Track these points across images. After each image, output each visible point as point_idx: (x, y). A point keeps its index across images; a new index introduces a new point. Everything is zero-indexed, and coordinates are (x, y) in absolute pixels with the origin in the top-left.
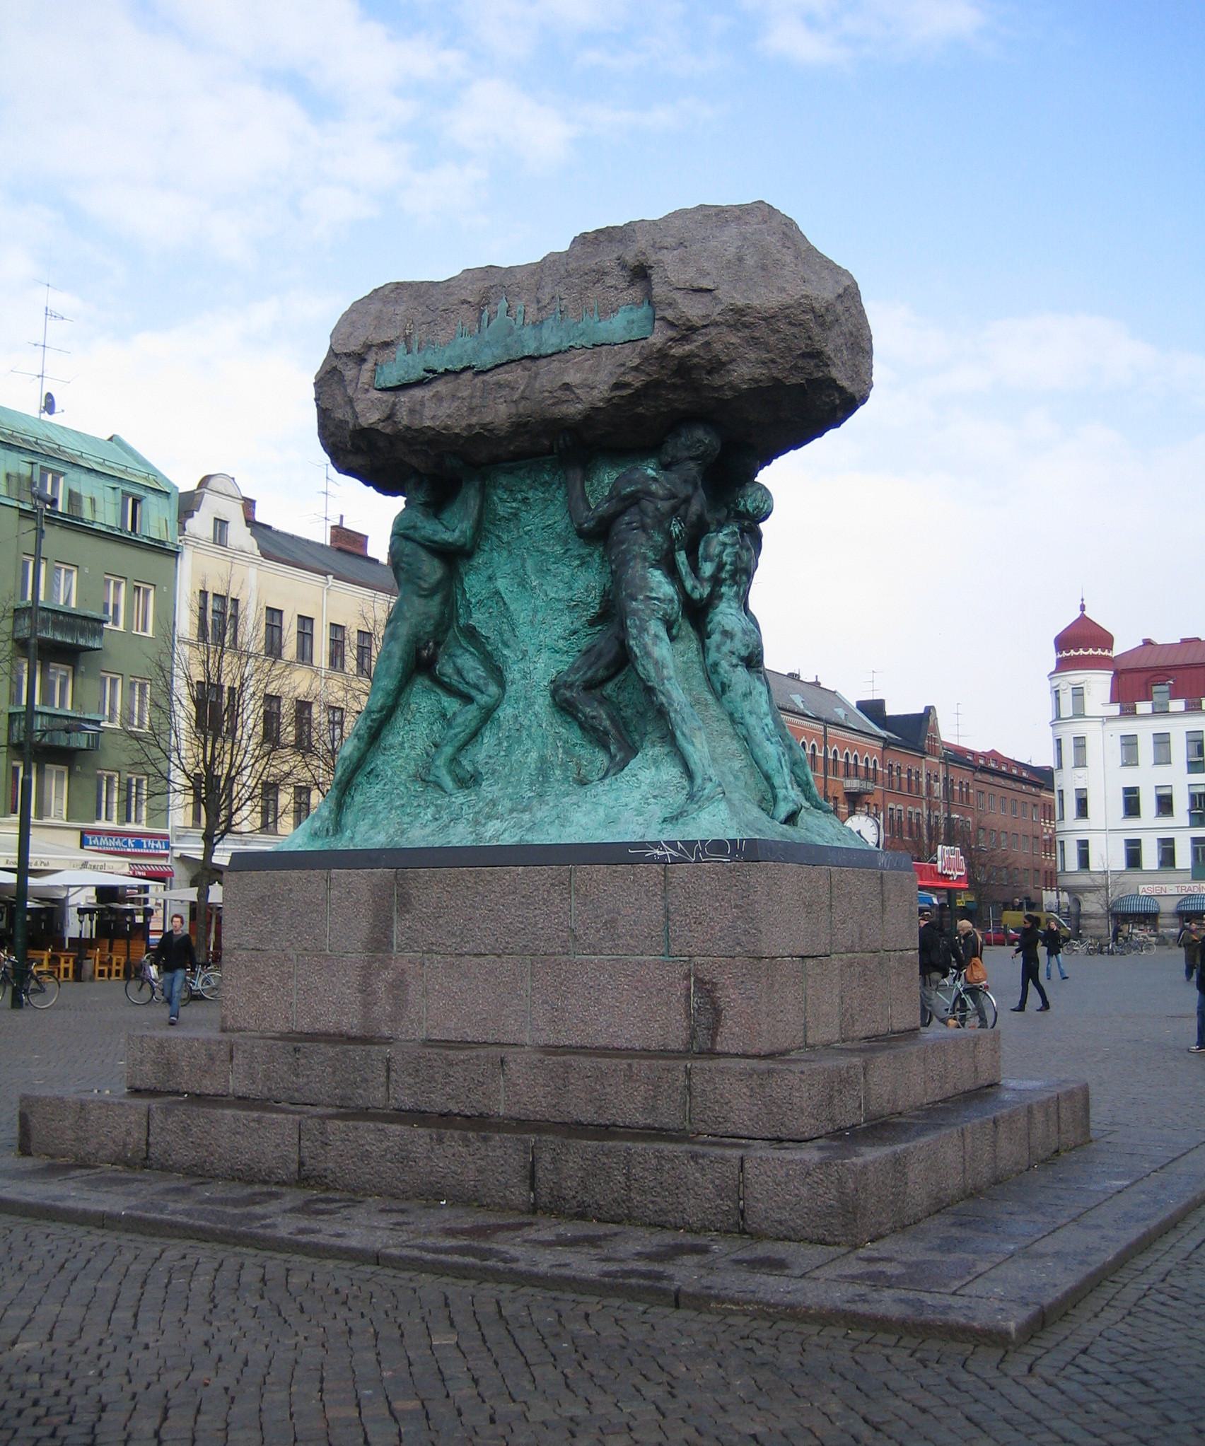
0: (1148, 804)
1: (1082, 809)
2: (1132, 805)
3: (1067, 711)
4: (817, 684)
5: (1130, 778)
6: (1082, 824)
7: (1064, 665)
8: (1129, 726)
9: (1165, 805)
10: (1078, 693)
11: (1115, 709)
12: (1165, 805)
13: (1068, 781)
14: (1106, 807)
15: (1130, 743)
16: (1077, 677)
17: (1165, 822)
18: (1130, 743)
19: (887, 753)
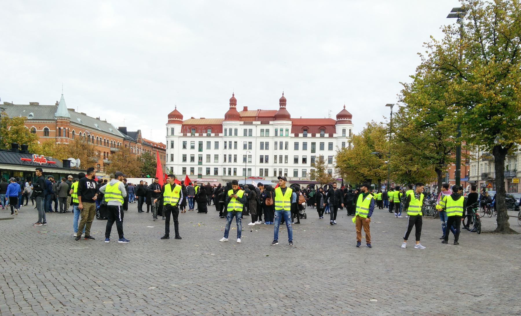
0: (188, 159)
1: (172, 160)
2: (185, 159)
3: (170, 134)
4: (105, 122)
5: (185, 152)
6: (172, 163)
7: (170, 122)
8: (185, 139)
9: (192, 159)
10: (173, 130)
11: (182, 134)
12: (192, 159)
13: (169, 151)
14: (178, 159)
17: (192, 163)
19: (125, 142)
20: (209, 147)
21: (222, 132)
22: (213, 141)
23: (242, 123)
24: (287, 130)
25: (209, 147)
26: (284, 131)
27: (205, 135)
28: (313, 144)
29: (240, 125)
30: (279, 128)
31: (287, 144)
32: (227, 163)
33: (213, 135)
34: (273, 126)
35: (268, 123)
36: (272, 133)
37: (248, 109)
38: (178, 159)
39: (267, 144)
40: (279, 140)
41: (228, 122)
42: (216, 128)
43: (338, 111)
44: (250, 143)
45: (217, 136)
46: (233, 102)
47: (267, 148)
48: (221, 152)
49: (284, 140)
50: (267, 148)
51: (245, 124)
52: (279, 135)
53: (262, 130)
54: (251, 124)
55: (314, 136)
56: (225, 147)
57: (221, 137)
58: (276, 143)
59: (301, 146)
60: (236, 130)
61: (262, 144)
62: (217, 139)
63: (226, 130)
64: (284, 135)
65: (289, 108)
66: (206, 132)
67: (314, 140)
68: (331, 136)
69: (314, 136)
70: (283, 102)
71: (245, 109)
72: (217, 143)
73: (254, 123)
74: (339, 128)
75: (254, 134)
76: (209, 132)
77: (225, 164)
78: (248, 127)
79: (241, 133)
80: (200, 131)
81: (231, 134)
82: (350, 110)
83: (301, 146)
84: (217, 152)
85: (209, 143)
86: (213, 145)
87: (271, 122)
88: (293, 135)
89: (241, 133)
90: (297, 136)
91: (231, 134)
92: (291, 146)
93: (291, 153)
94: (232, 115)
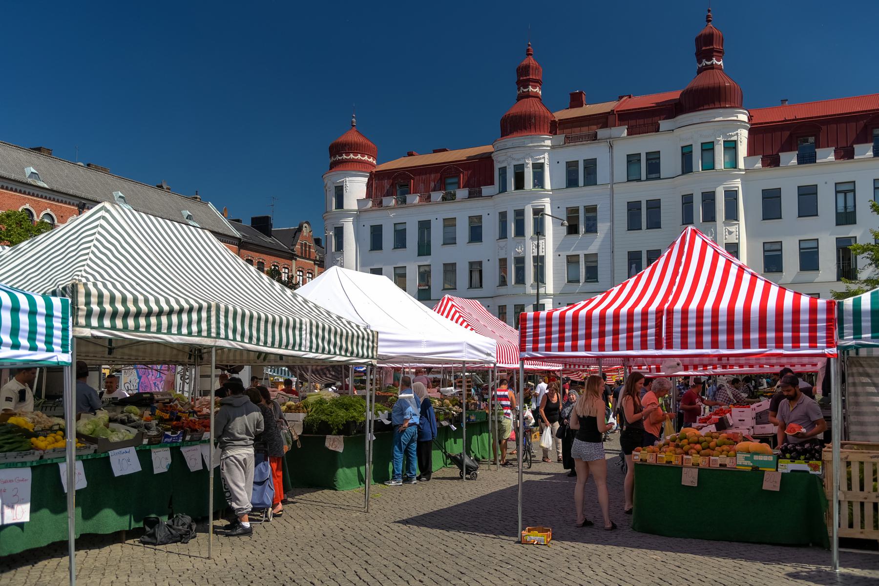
21: (492, 183)
28: (846, 190)
33: (462, 193)
35: (657, 130)
36: (670, 163)
39: (654, 206)
44: (591, 210)
45: (475, 194)
50: (655, 223)
55: (846, 154)
56: (503, 235)
58: (687, 201)
61: (633, 208)
62: (476, 207)
63: (503, 171)
67: (846, 171)
69: (846, 154)
73: (602, 133)
77: (503, 290)
85: (450, 223)
87: (664, 124)
90: (772, 161)
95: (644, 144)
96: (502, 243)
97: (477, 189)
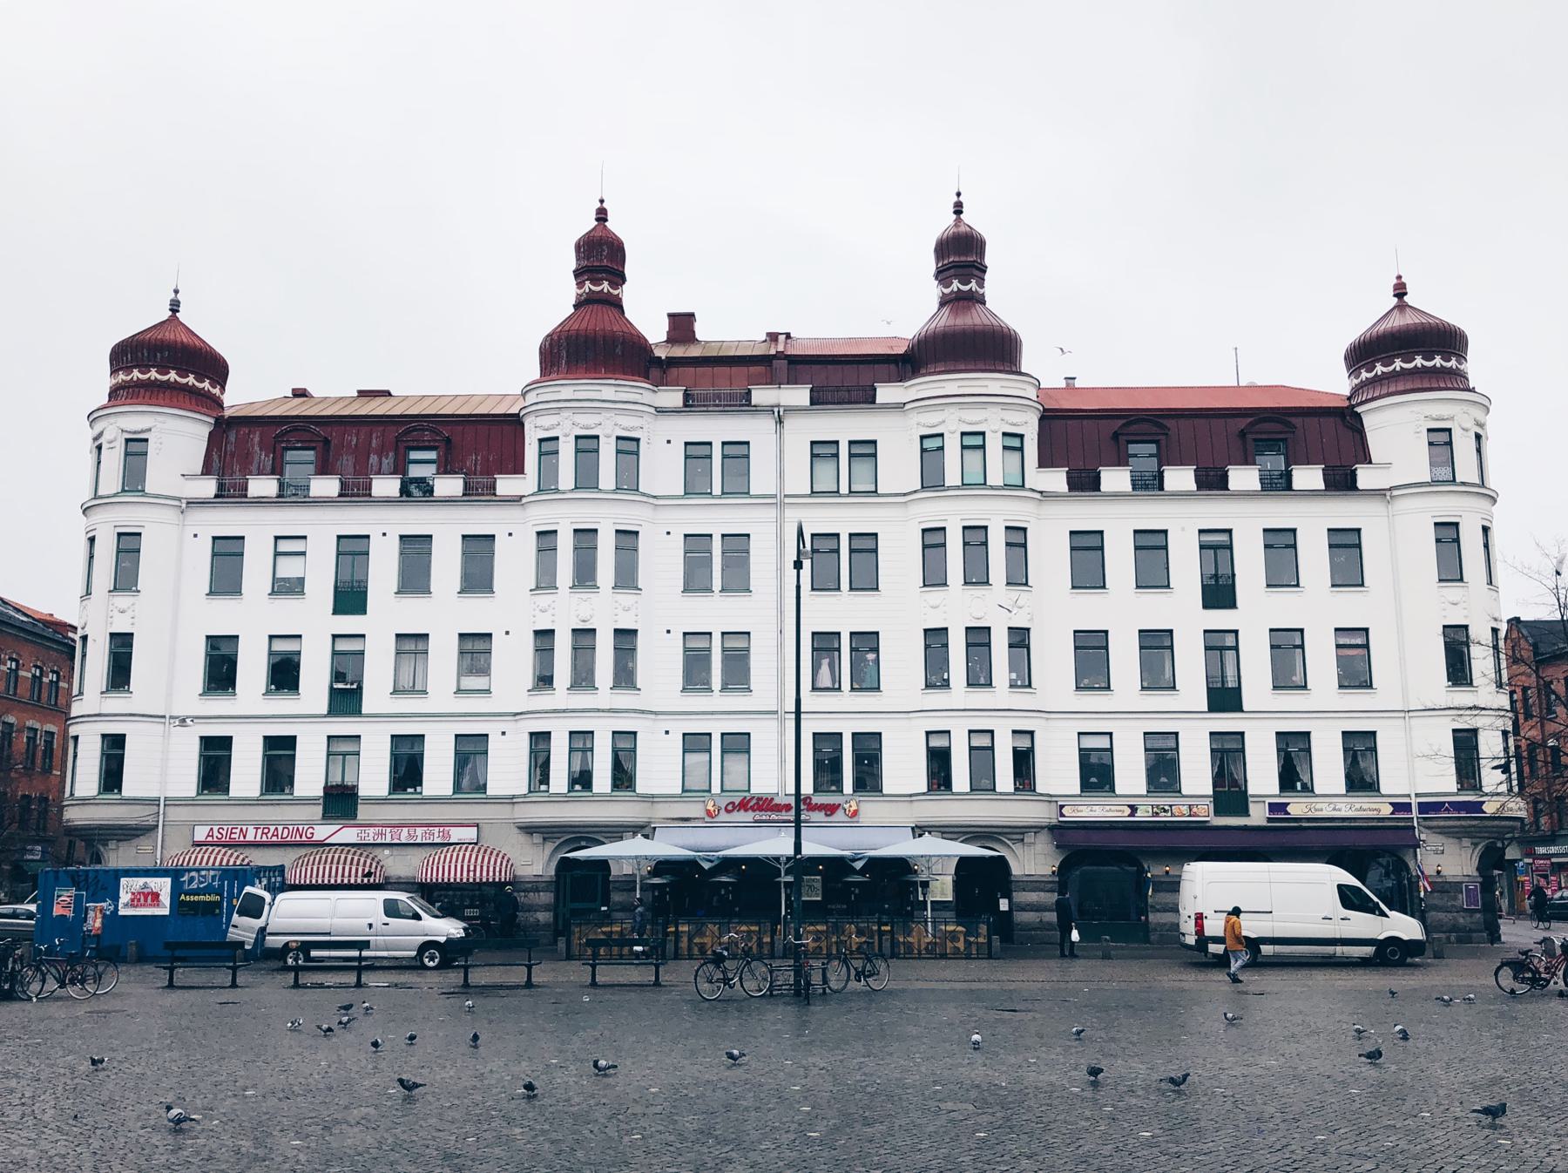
0: (252, 668)
1: (120, 674)
2: (221, 670)
3: (112, 481)
5: (223, 617)
6: (116, 703)
8: (229, 521)
9: (284, 674)
10: (136, 448)
11: (209, 487)
12: (284, 674)
14: (169, 673)
15: (228, 552)
16: (136, 419)
17: (283, 704)
18: (228, 552)
20: (414, 578)
21: (518, 468)
22: (447, 528)
23: (672, 397)
24: (1013, 441)
25: (414, 578)
26: (994, 445)
27: (385, 486)
28: (1217, 546)
29: (661, 411)
30: (952, 424)
31: (1017, 539)
32: (561, 694)
33: (448, 486)
34: (897, 424)
35: (869, 398)
36: (899, 465)
37: (701, 332)
38: (169, 673)
40: (953, 514)
41: (568, 390)
42: (479, 446)
43: (1367, 312)
45: (479, 491)
46: (601, 258)
47: (866, 581)
48: (511, 612)
49: (996, 515)
50: (866, 581)
51: (691, 403)
52: (952, 477)
53: (822, 451)
54: (742, 403)
55: (1212, 481)
57: (516, 500)
59: (1120, 558)
60: (629, 447)
62: (479, 519)
63: (549, 446)
64: (995, 478)
65: (1004, 298)
66: (399, 468)
67: (1215, 513)
68: (1341, 482)
69: (1212, 481)
70: (961, 256)
71: (682, 326)
72: (479, 549)
73: (761, 395)
74: (1396, 431)
75: (762, 478)
76: (415, 471)
77: (544, 701)
78: (716, 429)
79: (662, 467)
80: (347, 461)
81: (586, 479)
82: (1435, 302)
83: (1120, 558)
84: (476, 614)
85: (416, 548)
86: (446, 563)
87: (886, 393)
88: (1056, 480)
89: (662, 467)
90: (1084, 483)
91: (586, 479)
92: (1050, 556)
93: (1054, 609)
94: (594, 344)
95: (844, 426)
96: (544, 599)
97: (485, 480)
